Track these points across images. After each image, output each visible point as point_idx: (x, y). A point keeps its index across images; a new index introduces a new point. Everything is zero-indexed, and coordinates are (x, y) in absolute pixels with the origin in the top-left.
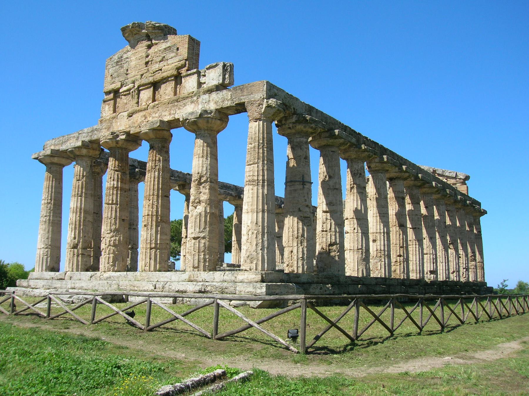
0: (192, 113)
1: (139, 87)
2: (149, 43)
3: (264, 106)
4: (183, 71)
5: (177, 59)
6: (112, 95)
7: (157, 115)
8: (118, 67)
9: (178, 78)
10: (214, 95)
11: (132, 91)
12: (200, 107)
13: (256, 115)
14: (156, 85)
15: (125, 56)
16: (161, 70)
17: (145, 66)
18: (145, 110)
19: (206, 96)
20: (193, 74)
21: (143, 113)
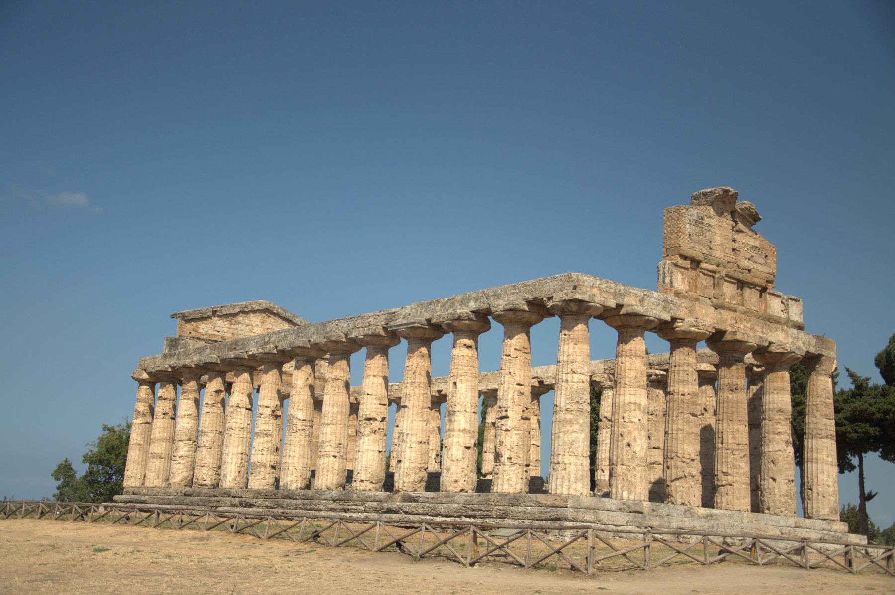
1: (727, 275)
3: (834, 366)
7: (749, 325)
8: (698, 229)
11: (717, 275)
12: (790, 340)
15: (706, 220)
16: (750, 271)
17: (732, 252)
18: (735, 311)
19: (795, 331)
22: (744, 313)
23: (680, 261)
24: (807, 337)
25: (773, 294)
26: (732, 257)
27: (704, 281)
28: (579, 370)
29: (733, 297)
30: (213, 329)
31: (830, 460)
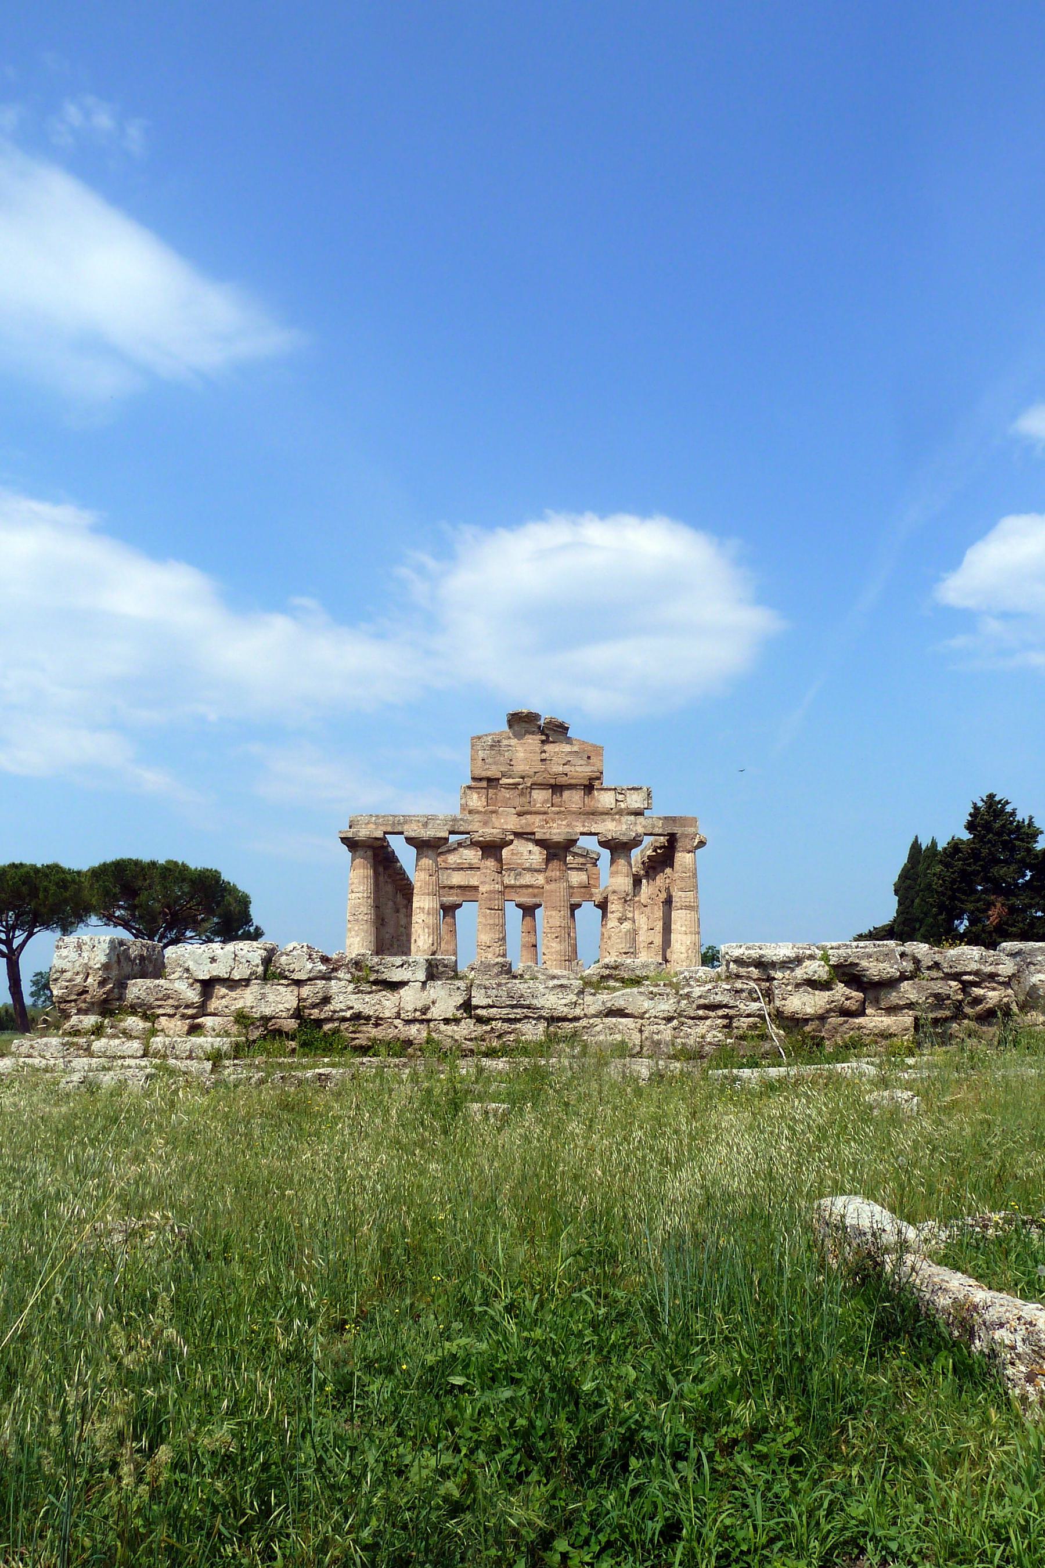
0: (624, 835)
2: (544, 738)
3: (697, 841)
4: (596, 783)
5: (588, 769)
6: (484, 784)
7: (564, 823)
8: (493, 752)
9: (589, 788)
10: (640, 819)
11: (520, 787)
12: (624, 827)
13: (689, 847)
14: (557, 788)
15: (505, 742)
18: (545, 813)
20: (610, 789)
21: (545, 817)
22: (558, 813)
23: (473, 784)
24: (650, 821)
25: (602, 789)
26: (540, 767)
27: (506, 794)
28: (355, 890)
29: (545, 801)
30: (461, 858)
31: (684, 929)
